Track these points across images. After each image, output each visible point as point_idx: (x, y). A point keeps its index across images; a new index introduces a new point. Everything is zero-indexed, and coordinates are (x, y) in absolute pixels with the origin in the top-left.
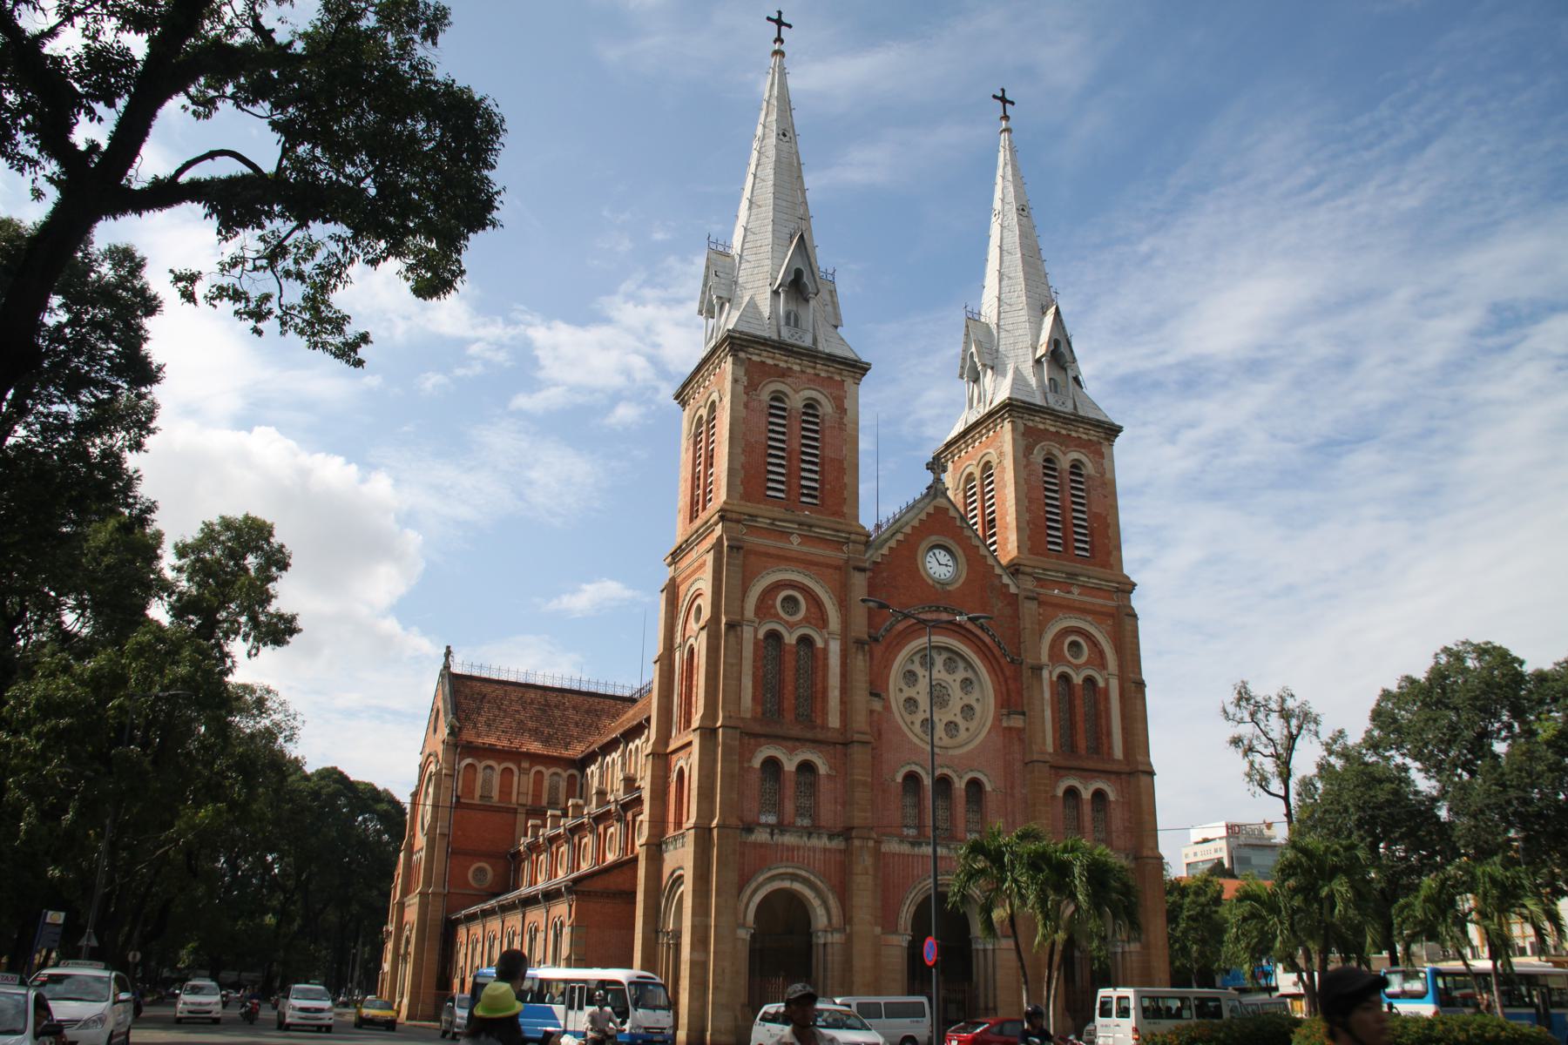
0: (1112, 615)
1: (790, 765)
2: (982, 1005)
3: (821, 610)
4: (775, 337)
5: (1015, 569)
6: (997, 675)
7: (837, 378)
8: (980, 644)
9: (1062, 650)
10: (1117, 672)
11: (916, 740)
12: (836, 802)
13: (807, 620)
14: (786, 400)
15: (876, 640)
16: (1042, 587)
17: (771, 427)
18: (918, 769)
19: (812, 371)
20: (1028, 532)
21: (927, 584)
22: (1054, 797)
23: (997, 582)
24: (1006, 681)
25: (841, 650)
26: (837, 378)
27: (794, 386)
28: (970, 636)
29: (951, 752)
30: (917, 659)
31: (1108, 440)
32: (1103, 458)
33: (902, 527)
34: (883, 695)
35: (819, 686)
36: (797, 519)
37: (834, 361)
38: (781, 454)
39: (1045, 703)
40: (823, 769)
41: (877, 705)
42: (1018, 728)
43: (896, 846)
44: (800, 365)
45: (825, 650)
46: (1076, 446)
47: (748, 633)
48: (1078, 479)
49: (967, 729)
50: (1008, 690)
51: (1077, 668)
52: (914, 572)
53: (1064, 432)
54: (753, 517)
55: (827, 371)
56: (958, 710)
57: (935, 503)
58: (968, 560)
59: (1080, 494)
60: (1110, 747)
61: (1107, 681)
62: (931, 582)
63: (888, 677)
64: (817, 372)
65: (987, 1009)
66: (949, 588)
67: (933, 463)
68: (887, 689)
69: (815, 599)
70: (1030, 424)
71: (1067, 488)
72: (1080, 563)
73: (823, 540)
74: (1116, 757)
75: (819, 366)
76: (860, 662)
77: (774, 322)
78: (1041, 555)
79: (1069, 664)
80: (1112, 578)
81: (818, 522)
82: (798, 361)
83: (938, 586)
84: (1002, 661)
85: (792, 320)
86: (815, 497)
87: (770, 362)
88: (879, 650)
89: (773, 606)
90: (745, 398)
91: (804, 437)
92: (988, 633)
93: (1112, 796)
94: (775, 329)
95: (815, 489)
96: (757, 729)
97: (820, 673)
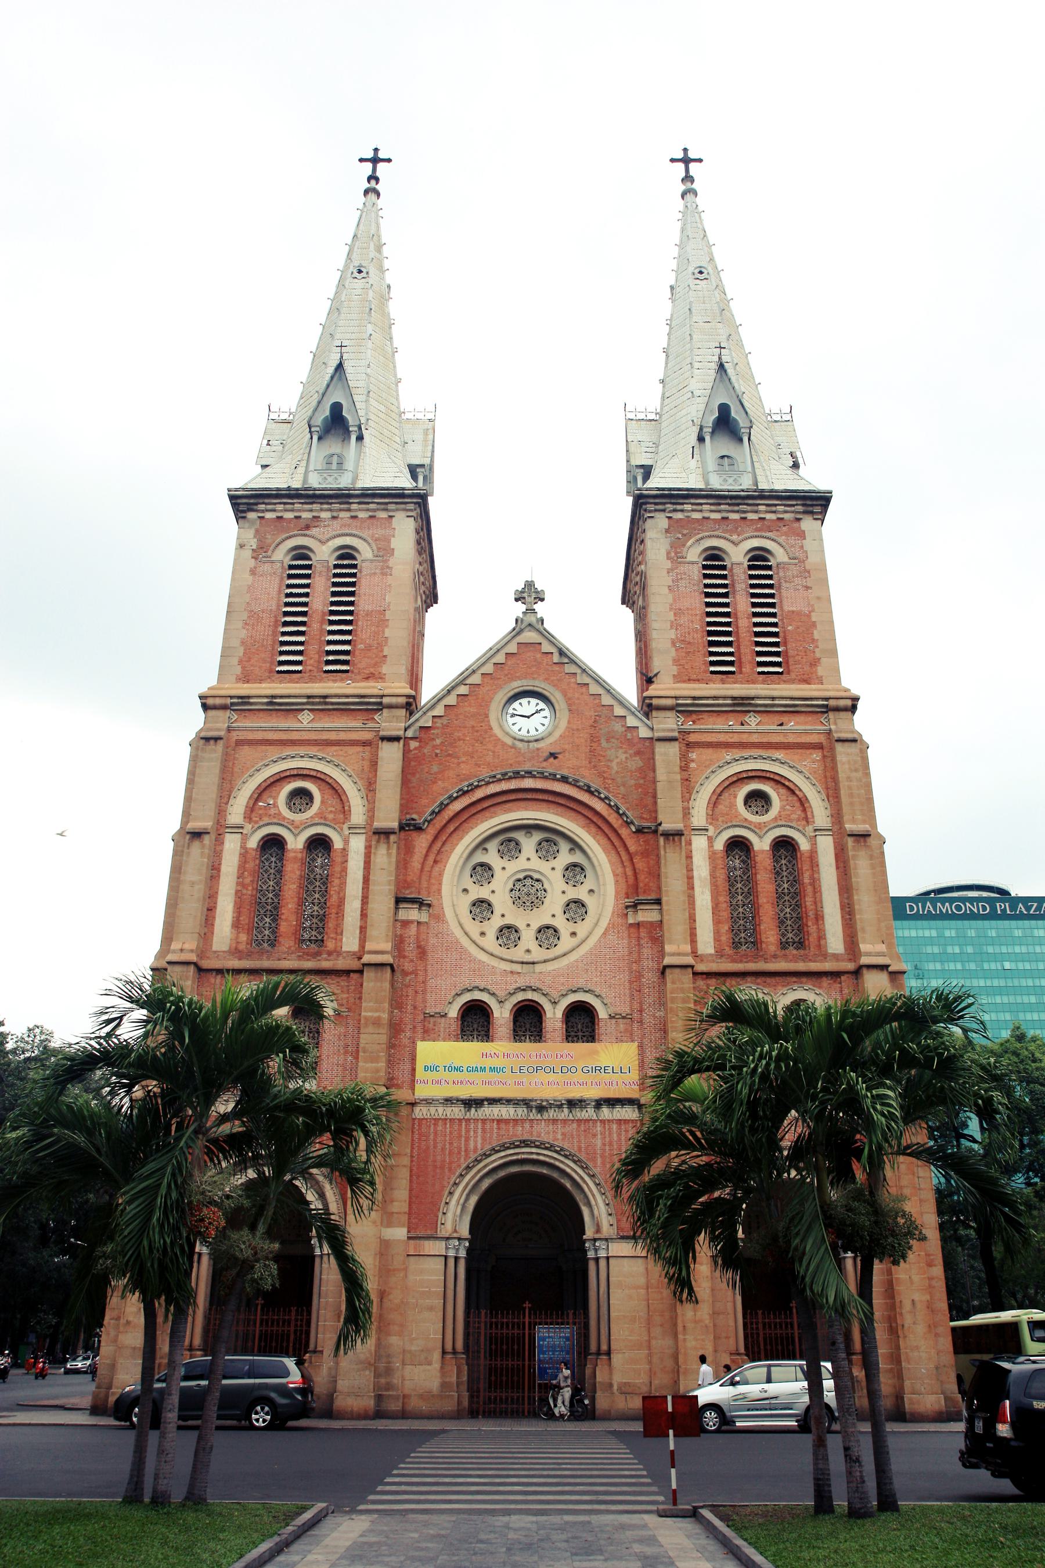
0: (819, 746)
2: (593, 1348)
4: (297, 484)
5: (648, 707)
6: (618, 853)
7: (383, 515)
8: (589, 814)
9: (733, 805)
10: (829, 825)
12: (346, 1052)
15: (418, 829)
17: (289, 591)
18: (484, 997)
19: (348, 514)
20: (673, 653)
21: (504, 744)
23: (618, 727)
24: (631, 860)
25: (368, 848)
27: (320, 537)
28: (572, 805)
29: (538, 968)
31: (805, 512)
33: (465, 679)
34: (428, 900)
35: (334, 899)
36: (309, 692)
37: (374, 496)
41: (412, 913)
42: (651, 923)
43: (440, 1110)
44: (330, 510)
45: (345, 851)
46: (757, 530)
47: (232, 844)
49: (574, 934)
50: (634, 869)
52: (483, 732)
54: (244, 699)
55: (368, 510)
56: (558, 910)
57: (519, 639)
58: (569, 705)
60: (821, 936)
61: (813, 841)
62: (509, 741)
63: (441, 875)
64: (353, 514)
65: (599, 1353)
67: (522, 592)
68: (439, 891)
69: (334, 788)
72: (764, 682)
75: (354, 506)
76: (385, 858)
77: (301, 470)
82: (325, 506)
83: (519, 745)
84: (624, 832)
86: (346, 663)
88: (422, 842)
89: (275, 805)
90: (252, 563)
91: (334, 594)
92: (600, 798)
95: (347, 653)
96: (237, 964)
97: (336, 882)
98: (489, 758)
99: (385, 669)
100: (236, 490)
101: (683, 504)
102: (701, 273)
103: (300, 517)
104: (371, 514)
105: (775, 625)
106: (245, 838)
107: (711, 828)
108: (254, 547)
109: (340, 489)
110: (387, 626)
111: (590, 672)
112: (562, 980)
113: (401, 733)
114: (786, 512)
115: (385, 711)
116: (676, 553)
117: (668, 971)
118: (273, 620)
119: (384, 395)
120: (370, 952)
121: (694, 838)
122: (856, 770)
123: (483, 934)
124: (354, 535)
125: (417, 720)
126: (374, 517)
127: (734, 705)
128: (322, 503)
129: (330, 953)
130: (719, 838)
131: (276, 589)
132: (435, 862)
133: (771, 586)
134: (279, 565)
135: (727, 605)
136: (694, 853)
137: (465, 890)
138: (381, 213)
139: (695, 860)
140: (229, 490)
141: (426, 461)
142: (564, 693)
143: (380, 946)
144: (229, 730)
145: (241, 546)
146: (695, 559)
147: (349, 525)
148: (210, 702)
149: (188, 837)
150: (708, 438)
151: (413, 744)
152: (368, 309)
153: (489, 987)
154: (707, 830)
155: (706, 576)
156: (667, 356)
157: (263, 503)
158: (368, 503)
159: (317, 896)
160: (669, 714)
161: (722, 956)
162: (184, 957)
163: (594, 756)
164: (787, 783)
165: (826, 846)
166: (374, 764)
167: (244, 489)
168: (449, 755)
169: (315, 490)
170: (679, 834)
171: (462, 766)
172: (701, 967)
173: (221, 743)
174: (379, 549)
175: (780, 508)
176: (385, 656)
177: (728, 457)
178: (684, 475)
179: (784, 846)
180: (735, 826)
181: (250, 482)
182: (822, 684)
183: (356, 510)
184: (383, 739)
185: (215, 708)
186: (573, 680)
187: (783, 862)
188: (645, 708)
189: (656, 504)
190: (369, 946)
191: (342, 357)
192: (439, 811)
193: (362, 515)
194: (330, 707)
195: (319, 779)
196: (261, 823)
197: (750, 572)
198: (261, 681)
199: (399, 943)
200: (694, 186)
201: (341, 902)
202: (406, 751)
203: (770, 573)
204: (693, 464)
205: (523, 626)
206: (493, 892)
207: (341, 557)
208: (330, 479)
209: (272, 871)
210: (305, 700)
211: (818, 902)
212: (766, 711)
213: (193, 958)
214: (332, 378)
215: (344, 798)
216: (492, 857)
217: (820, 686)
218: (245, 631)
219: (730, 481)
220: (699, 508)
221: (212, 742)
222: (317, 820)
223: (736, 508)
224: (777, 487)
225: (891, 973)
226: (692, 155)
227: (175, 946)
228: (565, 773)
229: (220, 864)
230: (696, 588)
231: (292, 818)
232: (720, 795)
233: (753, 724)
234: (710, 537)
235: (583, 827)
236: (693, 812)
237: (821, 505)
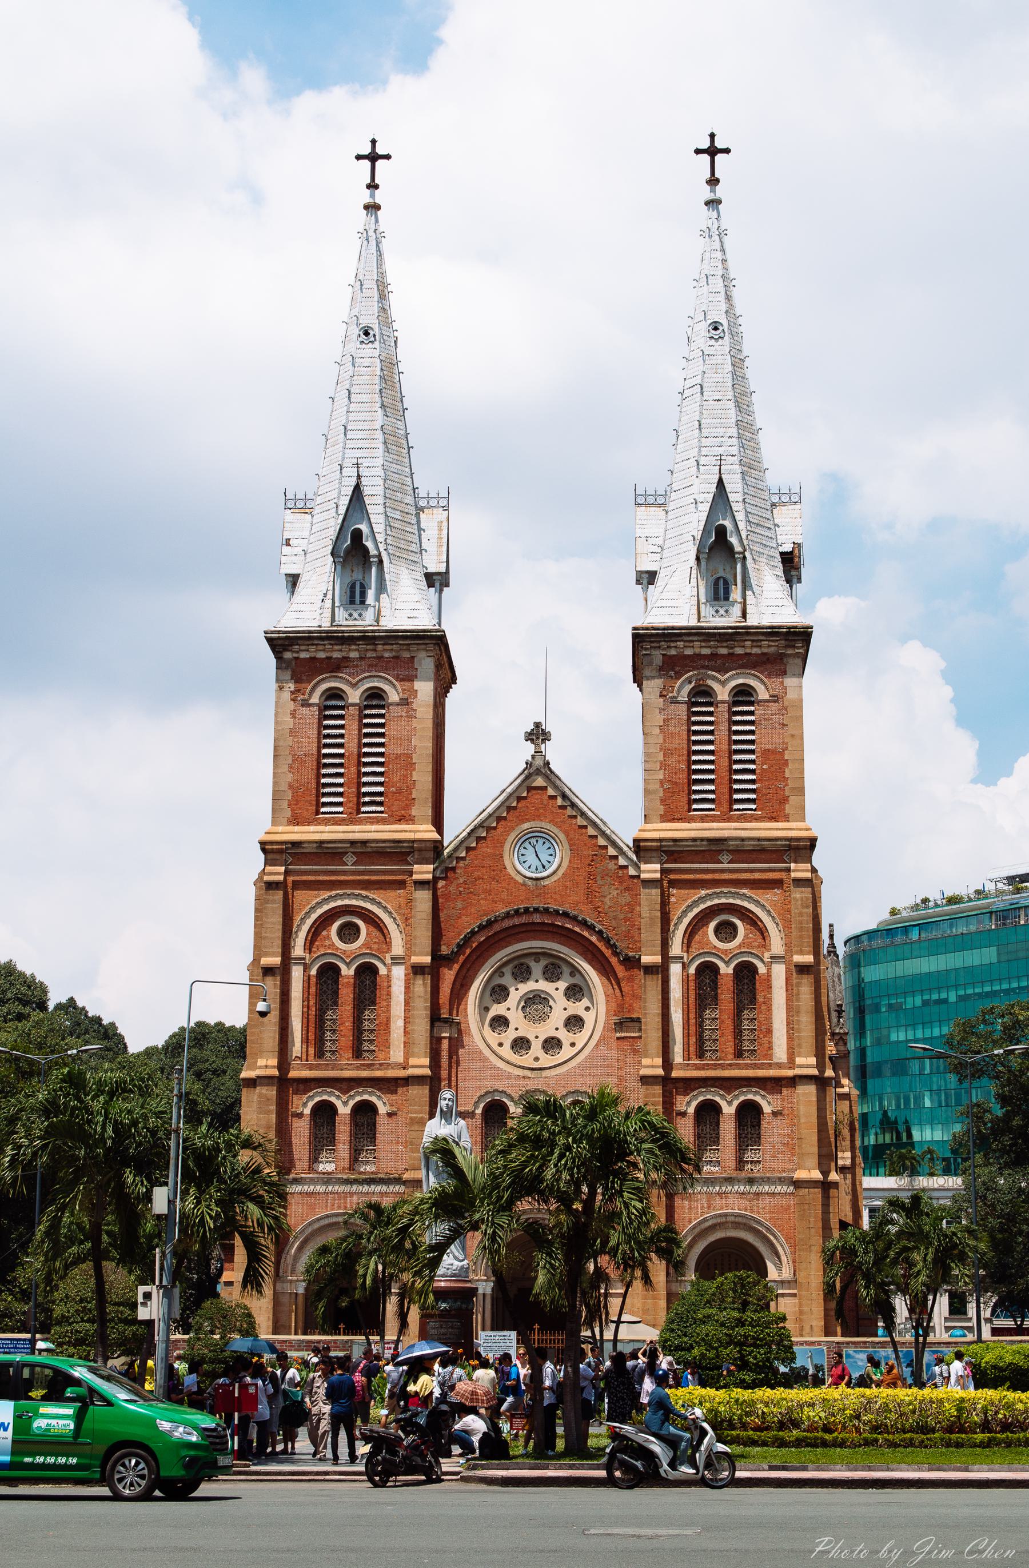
4: (326, 625)
5: (639, 846)
7: (406, 655)
9: (706, 934)
11: (500, 1064)
12: (398, 1143)
16: (675, 862)
20: (661, 794)
21: (516, 882)
26: (406, 655)
29: (545, 1073)
30: (508, 970)
31: (786, 647)
33: (484, 822)
34: (457, 1019)
39: (672, 1003)
40: (382, 1109)
48: (745, 708)
54: (296, 844)
56: (561, 1024)
62: (520, 879)
66: (546, 882)
67: (530, 734)
70: (673, 652)
75: (380, 647)
76: (422, 987)
77: (328, 603)
82: (354, 647)
84: (614, 960)
86: (380, 804)
87: (322, 655)
89: (329, 937)
90: (291, 706)
91: (367, 735)
97: (384, 1003)
98: (504, 895)
99: (414, 812)
100: (272, 632)
105: (753, 762)
108: (292, 689)
110: (414, 769)
111: (590, 814)
112: (563, 1083)
113: (430, 876)
114: (769, 646)
118: (315, 763)
120: (413, 1067)
122: (807, 907)
123: (501, 1045)
129: (381, 1065)
131: (316, 733)
133: (752, 723)
135: (710, 742)
140: (266, 633)
142: (567, 835)
147: (376, 665)
150: (703, 563)
153: (505, 1089)
154: (682, 958)
160: (654, 854)
163: (590, 894)
165: (779, 971)
166: (410, 901)
167: (279, 632)
168: (471, 893)
169: (343, 632)
171: (482, 902)
174: (404, 690)
185: (273, 851)
186: (574, 821)
187: (746, 981)
189: (652, 642)
191: (359, 477)
194: (369, 850)
196: (319, 953)
197: (735, 709)
198: (309, 823)
201: (388, 1019)
204: (690, 591)
205: (532, 771)
206: (509, 1009)
215: (385, 931)
216: (507, 980)
222: (364, 951)
228: (566, 908)
235: (581, 955)
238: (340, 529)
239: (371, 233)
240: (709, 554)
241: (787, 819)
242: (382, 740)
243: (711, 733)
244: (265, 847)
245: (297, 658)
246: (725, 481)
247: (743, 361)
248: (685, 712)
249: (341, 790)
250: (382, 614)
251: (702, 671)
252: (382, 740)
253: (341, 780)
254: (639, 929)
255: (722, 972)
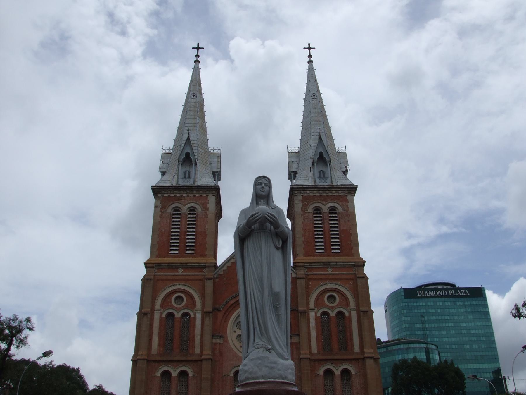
0: (352, 279)
1: (175, 374)
3: (193, 300)
4: (174, 184)
7: (205, 195)
10: (355, 307)
13: (186, 306)
14: (180, 210)
15: (219, 310)
17: (173, 223)
19: (192, 195)
22: (319, 375)
31: (348, 193)
32: (348, 203)
36: (182, 262)
38: (177, 234)
40: (191, 374)
41: (218, 341)
45: (195, 318)
47: (157, 316)
48: (334, 215)
51: (332, 309)
53: (325, 195)
54: (159, 264)
55: (199, 193)
59: (335, 222)
60: (352, 346)
61: (350, 313)
63: (227, 327)
64: (194, 195)
68: (226, 332)
69: (190, 296)
70: (306, 195)
71: (326, 221)
72: (334, 256)
73: (193, 268)
74: (355, 351)
75: (195, 192)
76: (207, 321)
77: (176, 178)
78: (311, 256)
79: (328, 307)
80: (351, 260)
81: (191, 261)
85: (187, 175)
87: (172, 195)
88: (220, 315)
89: (171, 302)
91: (189, 224)
93: (353, 372)
94: (175, 181)
99: (207, 253)
100: (154, 186)
101: (307, 191)
102: (314, 96)
103: (176, 196)
104: (200, 195)
106: (161, 314)
107: (316, 309)
109: (189, 186)
110: (207, 237)
113: (212, 277)
115: (207, 268)
116: (304, 209)
117: (302, 360)
119: (203, 145)
120: (205, 355)
121: (310, 312)
124: (195, 203)
125: (218, 271)
126: (201, 196)
127: (323, 265)
128: (183, 191)
130: (318, 312)
132: (225, 322)
134: (169, 214)
136: (310, 318)
137: (235, 332)
138: (200, 70)
139: (310, 320)
141: (219, 171)
143: (207, 353)
144: (154, 275)
145: (156, 207)
146: (311, 211)
148: (148, 265)
149: (142, 314)
150: (315, 165)
151: (217, 280)
152: (197, 111)
155: (315, 217)
156: (302, 129)
157: (164, 191)
158: (200, 191)
159: (185, 334)
160: (302, 268)
161: (320, 354)
162: (143, 357)
164: (341, 292)
165: (354, 314)
166: (204, 287)
167: (157, 186)
169: (181, 186)
170: (305, 312)
172: (313, 358)
173: (152, 280)
175: (340, 192)
176: (206, 248)
177: (322, 171)
178: (307, 178)
179: (340, 314)
180: (324, 308)
181: (158, 182)
182: (353, 256)
183: (195, 194)
184: (207, 279)
188: (294, 267)
190: (204, 353)
191: (189, 135)
192: (226, 304)
193: (197, 195)
194: (189, 267)
195: (186, 292)
196: (166, 309)
197: (329, 215)
199: (213, 350)
200: (312, 59)
202: (214, 283)
203: (336, 215)
204: (310, 174)
207: (190, 211)
208: (186, 181)
209: (170, 325)
210: (180, 265)
211: (351, 335)
212: (333, 267)
213: (146, 358)
214: (186, 142)
217: (353, 257)
218: (158, 238)
219: (323, 181)
220: (313, 192)
221: (149, 280)
223: (325, 192)
224: (339, 184)
225: (374, 359)
226: (311, 46)
227: (140, 353)
229: (153, 324)
230: (311, 221)
231: (176, 307)
232: (319, 297)
233: (330, 272)
234: (316, 202)
236: (310, 303)
237: (354, 190)
238: (182, 152)
239: (196, 68)
240: (317, 161)
241: (353, 255)
242: (195, 226)
243: (321, 224)
244: (147, 265)
245: (163, 196)
246: (321, 136)
247: (324, 106)
248: (311, 215)
249: (178, 245)
250: (196, 181)
251: (317, 201)
252: (195, 226)
253: (178, 241)
254: (297, 298)
255: (331, 315)
